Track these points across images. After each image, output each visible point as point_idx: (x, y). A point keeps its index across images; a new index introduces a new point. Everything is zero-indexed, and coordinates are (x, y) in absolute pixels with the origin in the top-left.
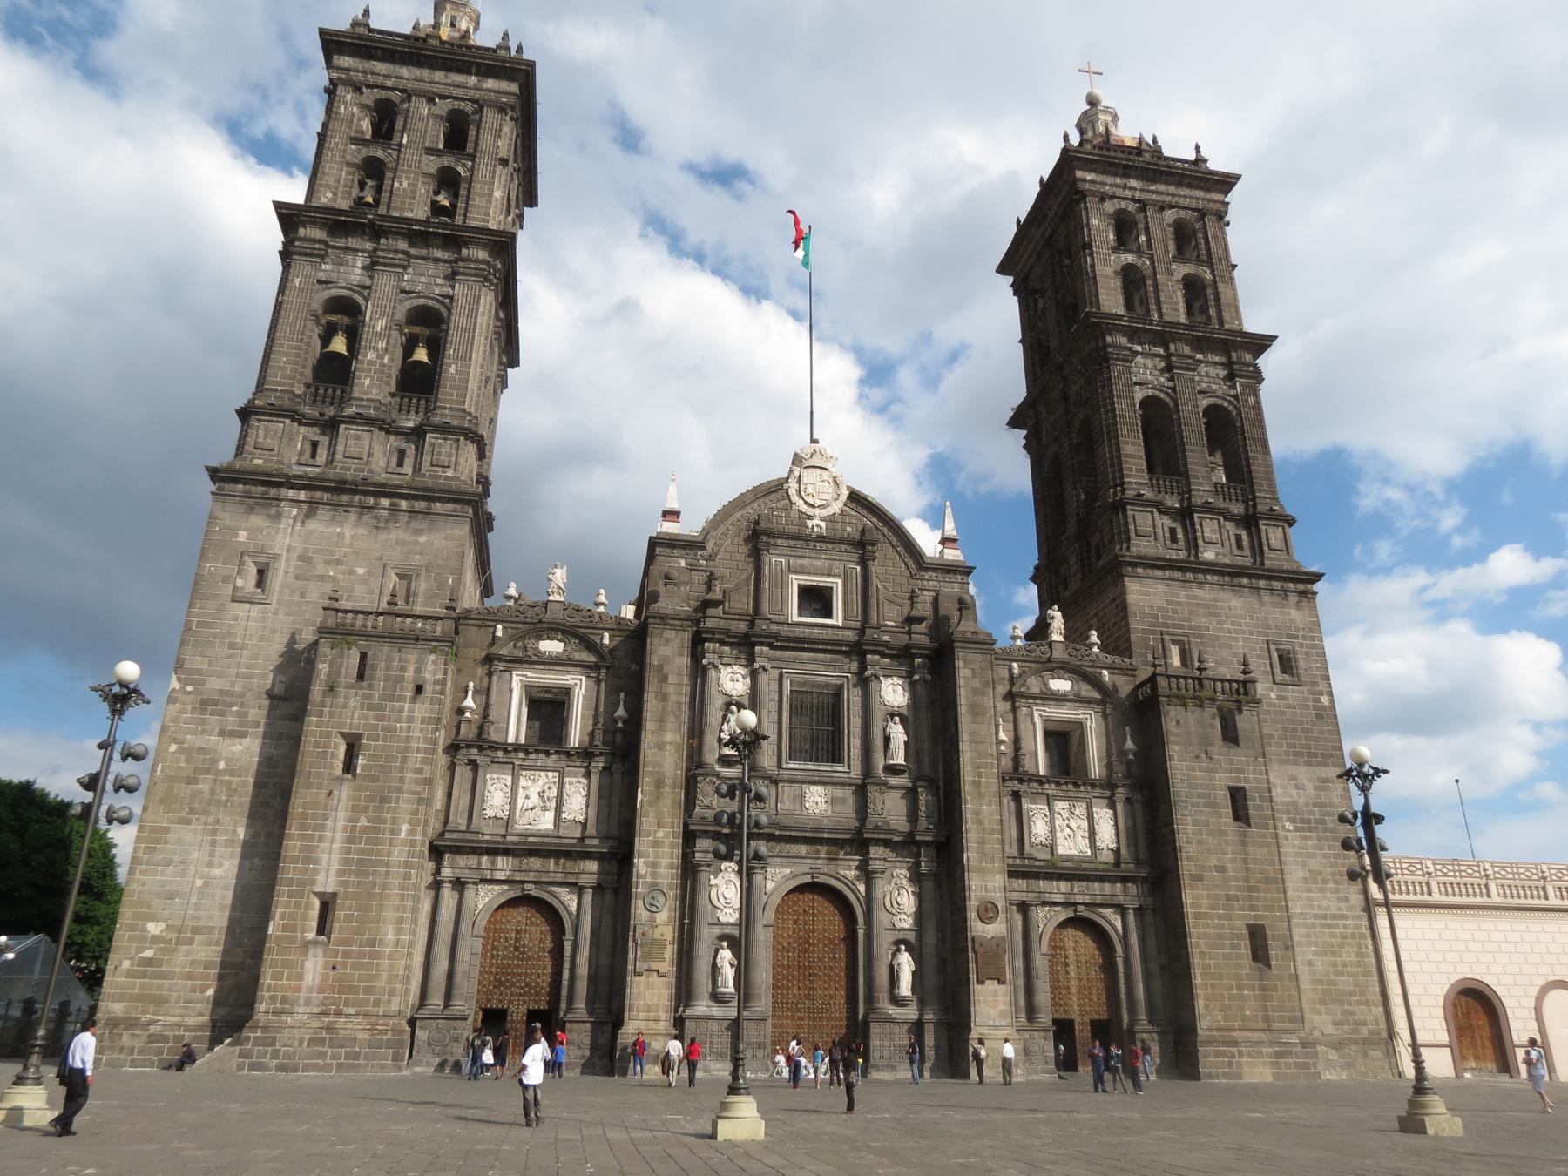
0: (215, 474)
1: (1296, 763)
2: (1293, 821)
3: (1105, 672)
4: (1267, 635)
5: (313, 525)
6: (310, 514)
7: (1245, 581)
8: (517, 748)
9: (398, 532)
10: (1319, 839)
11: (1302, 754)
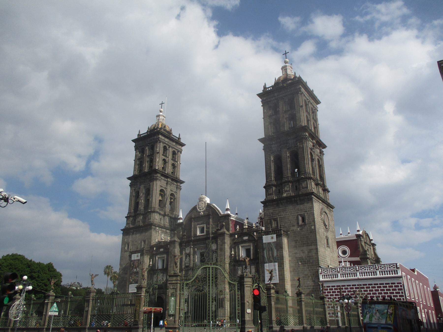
0: (122, 230)
1: (303, 246)
2: (301, 262)
3: (255, 233)
4: (298, 213)
5: (134, 236)
6: (133, 234)
7: (293, 199)
8: (158, 269)
9: (143, 234)
10: (308, 266)
11: (305, 244)
